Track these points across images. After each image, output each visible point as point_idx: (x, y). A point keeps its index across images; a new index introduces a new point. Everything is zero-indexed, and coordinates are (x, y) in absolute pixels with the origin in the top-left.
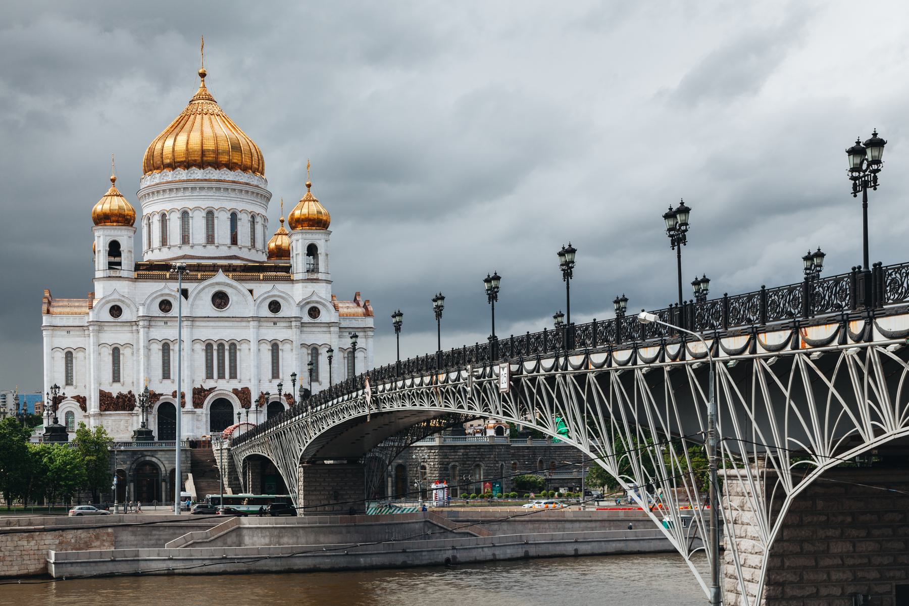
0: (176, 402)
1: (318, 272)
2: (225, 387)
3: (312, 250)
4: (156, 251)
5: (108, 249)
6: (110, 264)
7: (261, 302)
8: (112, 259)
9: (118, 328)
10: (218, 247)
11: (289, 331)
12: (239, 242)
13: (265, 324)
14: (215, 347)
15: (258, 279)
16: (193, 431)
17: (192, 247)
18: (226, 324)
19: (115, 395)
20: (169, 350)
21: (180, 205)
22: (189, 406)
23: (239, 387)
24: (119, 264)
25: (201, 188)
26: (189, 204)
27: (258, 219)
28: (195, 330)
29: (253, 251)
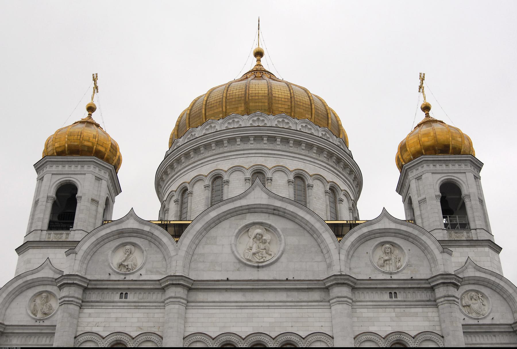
11: (431, 312)
13: (368, 296)
18: (271, 296)
21: (206, 170)
28: (194, 314)
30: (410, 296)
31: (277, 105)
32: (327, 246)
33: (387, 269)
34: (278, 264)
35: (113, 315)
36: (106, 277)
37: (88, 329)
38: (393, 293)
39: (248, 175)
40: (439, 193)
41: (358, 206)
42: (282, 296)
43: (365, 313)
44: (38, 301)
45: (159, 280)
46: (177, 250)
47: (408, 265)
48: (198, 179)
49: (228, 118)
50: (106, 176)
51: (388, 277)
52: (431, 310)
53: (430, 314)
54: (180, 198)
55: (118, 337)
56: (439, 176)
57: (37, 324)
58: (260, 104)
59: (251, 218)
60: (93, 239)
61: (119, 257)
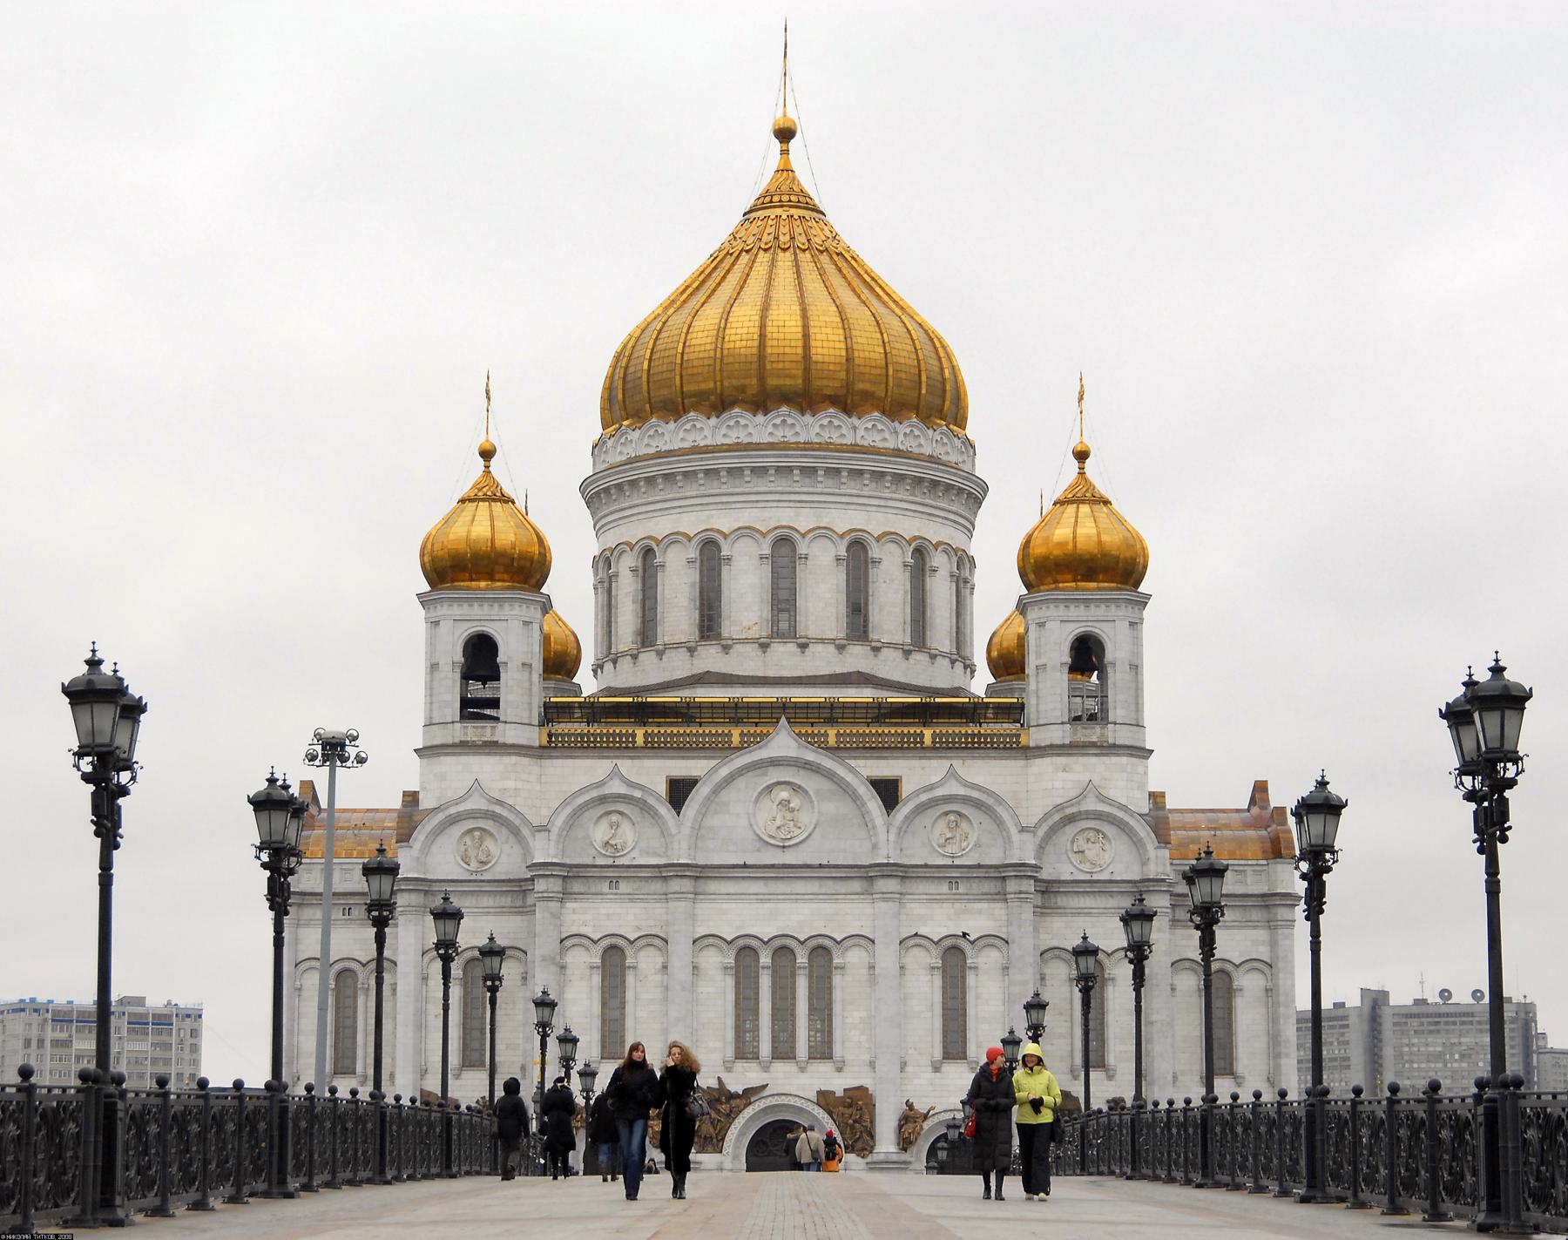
2: (795, 1085)
3: (1086, 655)
4: (625, 663)
5: (459, 657)
6: (466, 703)
7: (909, 819)
8: (476, 689)
10: (803, 647)
11: (998, 909)
12: (873, 636)
14: (765, 959)
15: (912, 747)
17: (726, 649)
18: (800, 887)
20: (623, 968)
23: (838, 1084)
24: (494, 703)
25: (760, 471)
26: (723, 521)
28: (703, 909)
29: (919, 658)
30: (976, 887)
31: (819, 383)
32: (872, 820)
33: (949, 849)
35: (603, 911)
36: (589, 861)
37: (574, 931)
38: (953, 882)
39: (767, 551)
41: (973, 551)
42: (813, 887)
43: (915, 908)
44: (467, 839)
46: (679, 825)
47: (977, 845)
49: (725, 415)
50: (534, 613)
51: (949, 862)
52: (999, 905)
53: (997, 912)
54: (640, 564)
55: (614, 940)
56: (1071, 626)
57: (473, 877)
58: (788, 382)
59: (775, 775)
60: (569, 810)
61: (600, 833)
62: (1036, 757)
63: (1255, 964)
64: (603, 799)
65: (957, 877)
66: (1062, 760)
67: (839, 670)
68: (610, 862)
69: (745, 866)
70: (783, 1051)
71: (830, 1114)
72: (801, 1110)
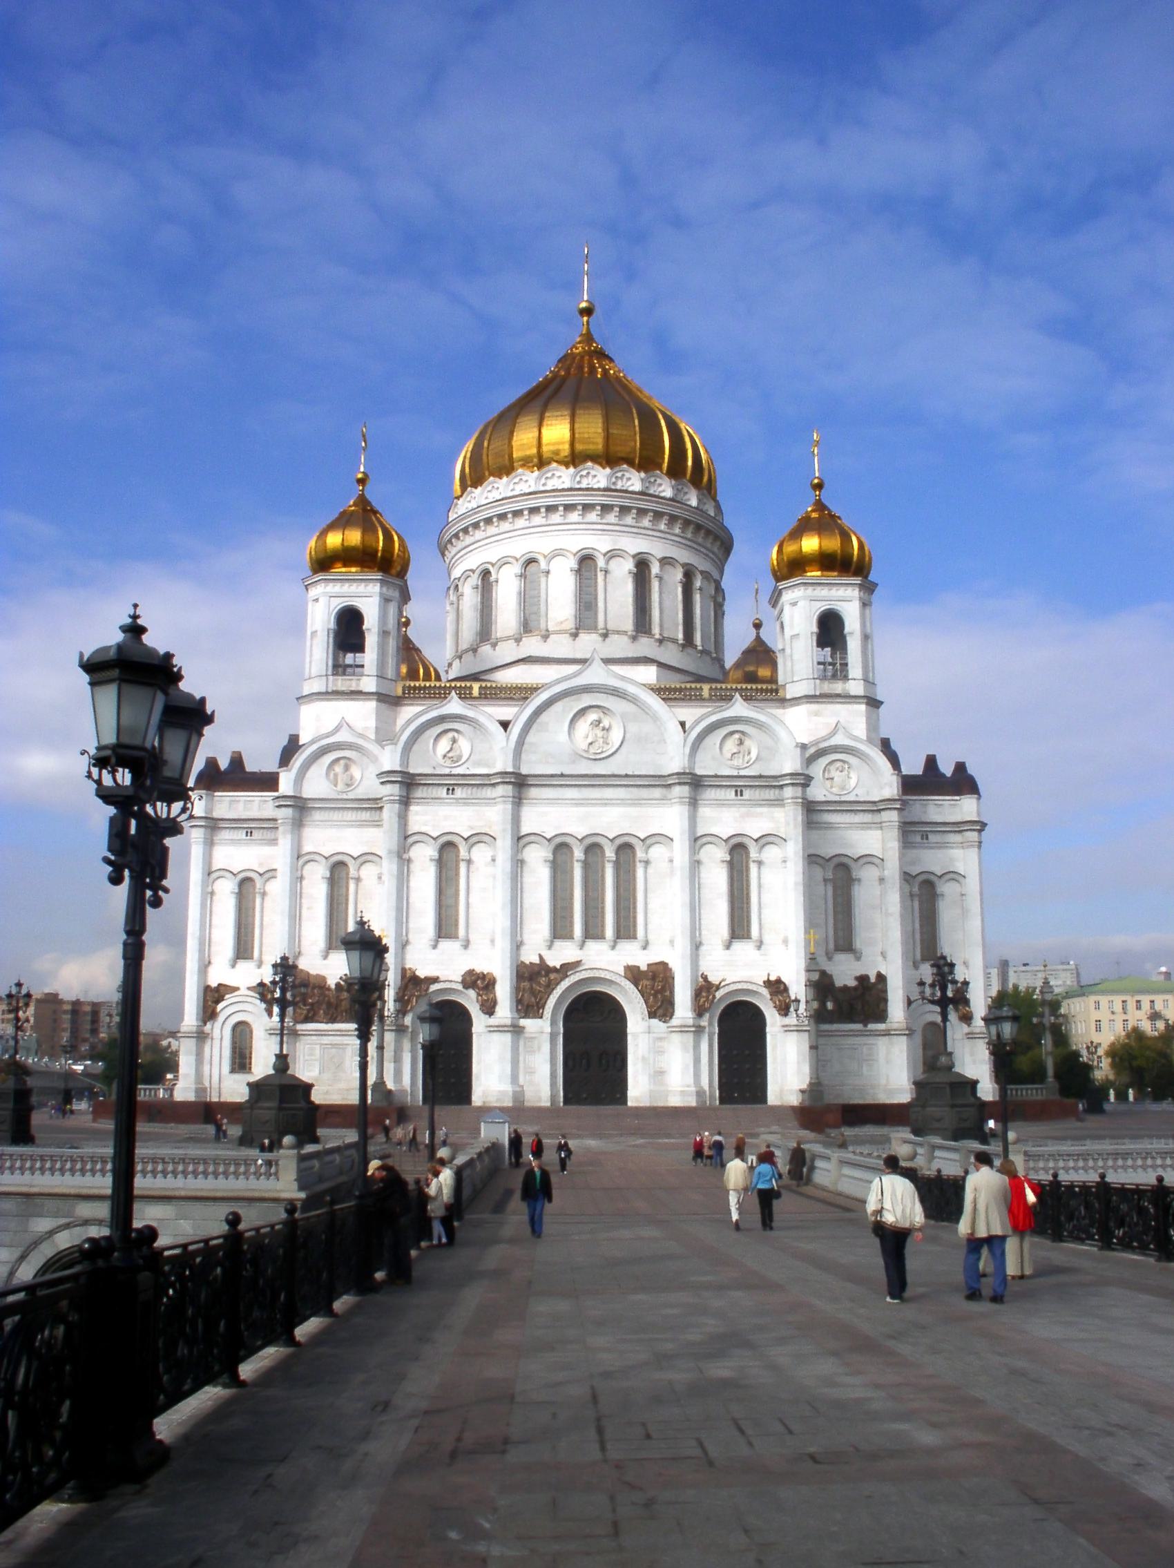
0: (470, 1001)
1: (845, 678)
2: (605, 961)
3: (830, 629)
5: (332, 625)
8: (349, 658)
9: (350, 816)
10: (605, 636)
12: (656, 630)
16: (514, 1078)
17: (546, 637)
18: (609, 793)
19: (332, 982)
22: (504, 1010)
23: (643, 961)
27: (698, 583)
29: (690, 650)
30: (757, 794)
34: (617, 756)
39: (572, 563)
40: (815, 629)
45: (488, 775)
48: (504, 562)
50: (396, 594)
56: (819, 604)
58: (591, 447)
59: (587, 700)
62: (792, 706)
63: (952, 876)
64: (442, 719)
65: (739, 785)
66: (814, 707)
67: (630, 655)
68: (447, 771)
69: (562, 775)
70: (593, 932)
71: (636, 985)
72: (611, 982)
